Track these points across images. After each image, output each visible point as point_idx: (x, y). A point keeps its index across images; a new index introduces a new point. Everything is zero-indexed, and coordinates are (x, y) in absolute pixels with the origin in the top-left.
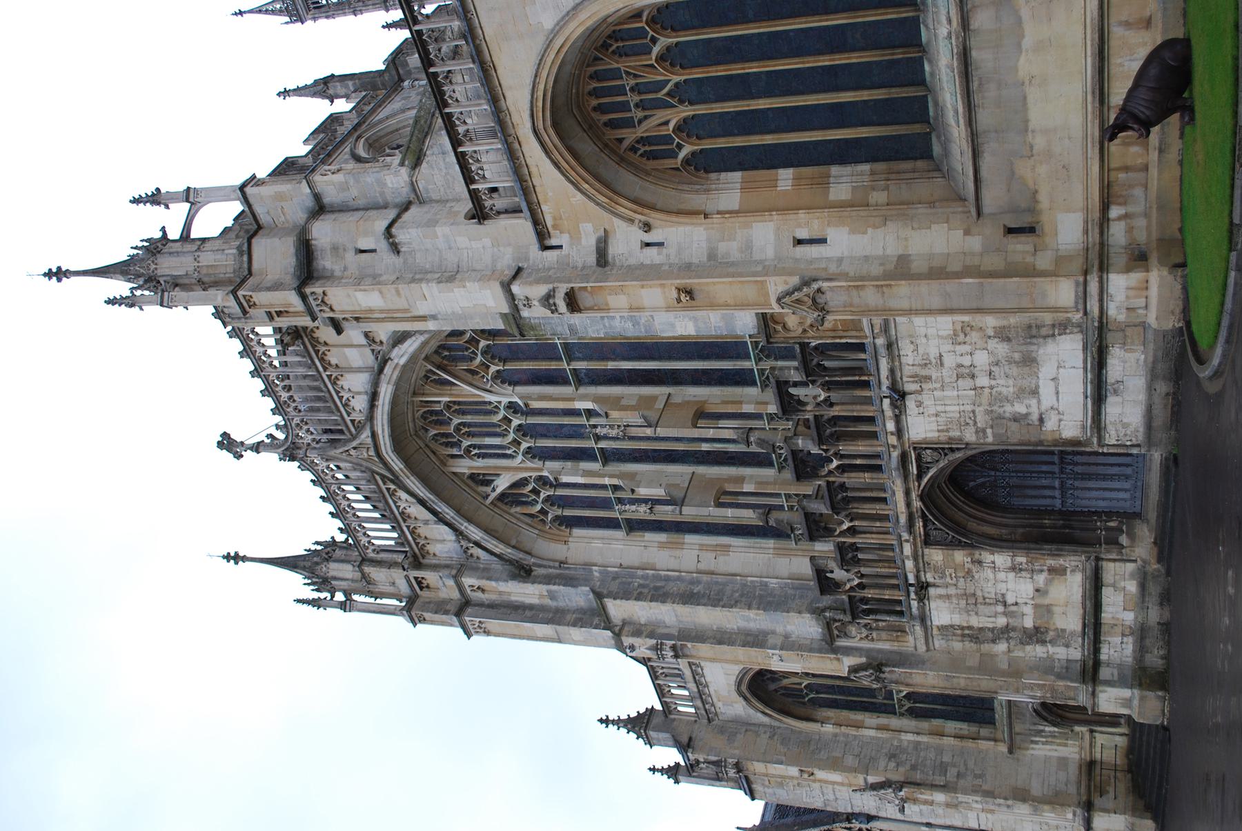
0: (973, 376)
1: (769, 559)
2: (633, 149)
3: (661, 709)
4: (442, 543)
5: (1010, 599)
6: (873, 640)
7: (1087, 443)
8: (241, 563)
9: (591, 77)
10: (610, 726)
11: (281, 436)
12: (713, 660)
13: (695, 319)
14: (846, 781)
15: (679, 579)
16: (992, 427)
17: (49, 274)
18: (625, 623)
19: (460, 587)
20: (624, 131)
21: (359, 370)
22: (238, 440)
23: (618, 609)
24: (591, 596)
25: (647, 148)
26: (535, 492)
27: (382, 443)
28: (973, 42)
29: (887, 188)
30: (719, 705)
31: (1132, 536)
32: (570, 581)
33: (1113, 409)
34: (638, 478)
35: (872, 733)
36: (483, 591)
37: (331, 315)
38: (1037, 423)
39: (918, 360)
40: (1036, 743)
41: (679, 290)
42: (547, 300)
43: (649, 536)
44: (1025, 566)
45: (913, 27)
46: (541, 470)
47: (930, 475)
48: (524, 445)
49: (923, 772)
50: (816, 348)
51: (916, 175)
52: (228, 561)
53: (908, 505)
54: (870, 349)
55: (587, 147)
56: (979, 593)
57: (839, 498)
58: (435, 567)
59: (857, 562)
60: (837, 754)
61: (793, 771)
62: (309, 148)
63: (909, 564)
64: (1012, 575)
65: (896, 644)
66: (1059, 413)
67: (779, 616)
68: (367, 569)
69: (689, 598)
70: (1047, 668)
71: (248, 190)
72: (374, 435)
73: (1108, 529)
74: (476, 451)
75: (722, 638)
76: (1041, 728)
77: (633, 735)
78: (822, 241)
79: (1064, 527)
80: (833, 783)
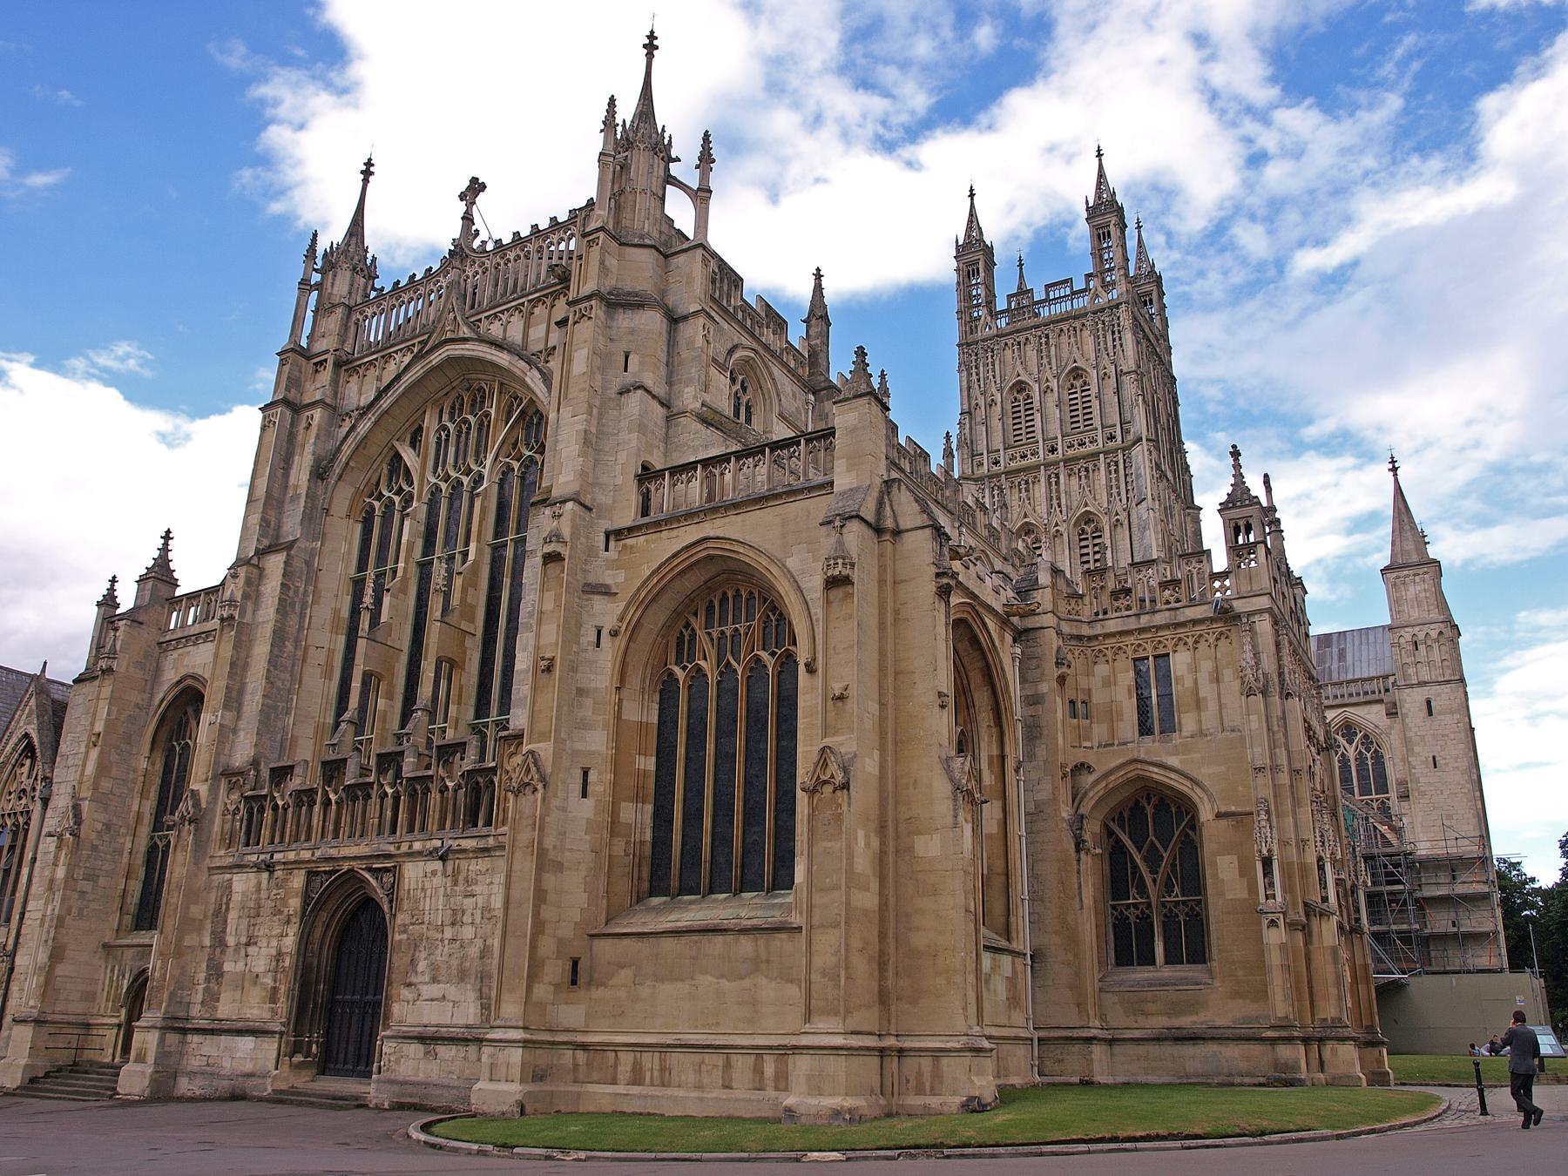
0: (453, 924)
1: (314, 718)
2: (687, 625)
3: (177, 595)
4: (358, 392)
5: (252, 950)
6: (224, 815)
7: (387, 1027)
8: (362, 177)
9: (751, 593)
10: (162, 541)
11: (476, 244)
12: (216, 656)
13: (527, 671)
14: (85, 779)
15: (301, 628)
16: (408, 939)
17: (652, 37)
18: (261, 570)
19: (313, 405)
20: (703, 618)
21: (525, 335)
22: (478, 200)
23: (275, 563)
24: (291, 538)
25: (687, 638)
26: (400, 491)
27: (457, 347)
28: (730, 938)
29: (627, 855)
30: (175, 655)
31: (300, 1066)
32: (308, 518)
33: (415, 1049)
34: (401, 596)
35: (135, 808)
36: (307, 428)
37: (571, 322)
38: (408, 981)
39: (473, 875)
40: (112, 970)
41: (553, 659)
42: (556, 536)
43: (348, 600)
44: (281, 965)
45: (756, 887)
46: (419, 500)
47: (371, 879)
48: (443, 486)
49: (89, 856)
50: (492, 782)
51: (635, 882)
52: (365, 164)
53: (345, 858)
54: (485, 831)
55: (691, 583)
56: (260, 920)
57: (359, 792)
58: (335, 382)
59: (299, 805)
60: (114, 772)
61: (99, 727)
62: (752, 302)
63: (291, 856)
64: (274, 952)
65: (219, 838)
66: (415, 1001)
67: (254, 726)
68: (340, 310)
69: (279, 635)
70: (184, 982)
71: (700, 251)
72: (465, 340)
73: (310, 1044)
74: (444, 437)
75: (238, 667)
76: (127, 976)
77: (150, 563)
78: (584, 795)
79: (315, 1004)
80: (84, 766)
